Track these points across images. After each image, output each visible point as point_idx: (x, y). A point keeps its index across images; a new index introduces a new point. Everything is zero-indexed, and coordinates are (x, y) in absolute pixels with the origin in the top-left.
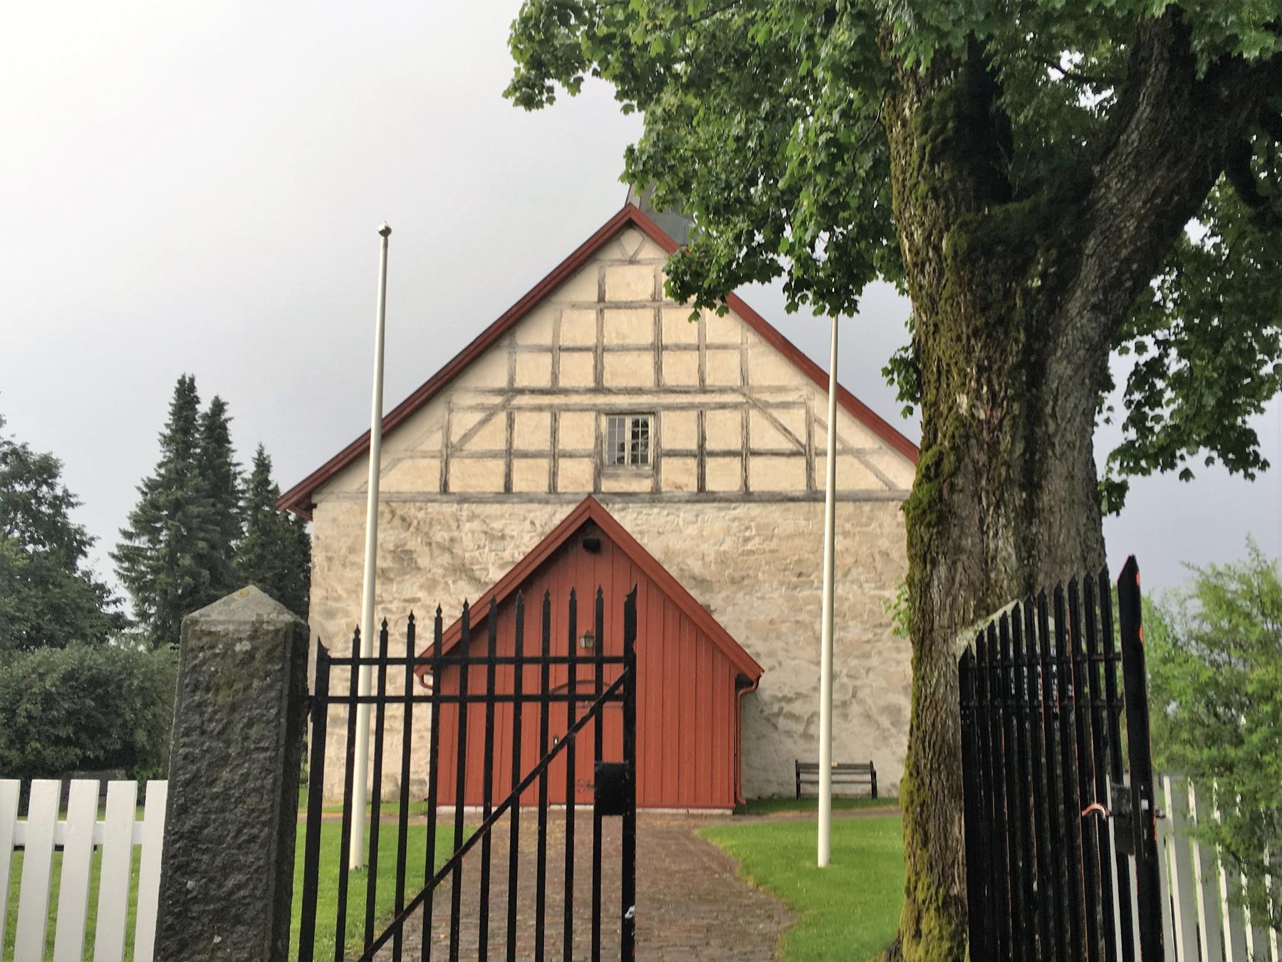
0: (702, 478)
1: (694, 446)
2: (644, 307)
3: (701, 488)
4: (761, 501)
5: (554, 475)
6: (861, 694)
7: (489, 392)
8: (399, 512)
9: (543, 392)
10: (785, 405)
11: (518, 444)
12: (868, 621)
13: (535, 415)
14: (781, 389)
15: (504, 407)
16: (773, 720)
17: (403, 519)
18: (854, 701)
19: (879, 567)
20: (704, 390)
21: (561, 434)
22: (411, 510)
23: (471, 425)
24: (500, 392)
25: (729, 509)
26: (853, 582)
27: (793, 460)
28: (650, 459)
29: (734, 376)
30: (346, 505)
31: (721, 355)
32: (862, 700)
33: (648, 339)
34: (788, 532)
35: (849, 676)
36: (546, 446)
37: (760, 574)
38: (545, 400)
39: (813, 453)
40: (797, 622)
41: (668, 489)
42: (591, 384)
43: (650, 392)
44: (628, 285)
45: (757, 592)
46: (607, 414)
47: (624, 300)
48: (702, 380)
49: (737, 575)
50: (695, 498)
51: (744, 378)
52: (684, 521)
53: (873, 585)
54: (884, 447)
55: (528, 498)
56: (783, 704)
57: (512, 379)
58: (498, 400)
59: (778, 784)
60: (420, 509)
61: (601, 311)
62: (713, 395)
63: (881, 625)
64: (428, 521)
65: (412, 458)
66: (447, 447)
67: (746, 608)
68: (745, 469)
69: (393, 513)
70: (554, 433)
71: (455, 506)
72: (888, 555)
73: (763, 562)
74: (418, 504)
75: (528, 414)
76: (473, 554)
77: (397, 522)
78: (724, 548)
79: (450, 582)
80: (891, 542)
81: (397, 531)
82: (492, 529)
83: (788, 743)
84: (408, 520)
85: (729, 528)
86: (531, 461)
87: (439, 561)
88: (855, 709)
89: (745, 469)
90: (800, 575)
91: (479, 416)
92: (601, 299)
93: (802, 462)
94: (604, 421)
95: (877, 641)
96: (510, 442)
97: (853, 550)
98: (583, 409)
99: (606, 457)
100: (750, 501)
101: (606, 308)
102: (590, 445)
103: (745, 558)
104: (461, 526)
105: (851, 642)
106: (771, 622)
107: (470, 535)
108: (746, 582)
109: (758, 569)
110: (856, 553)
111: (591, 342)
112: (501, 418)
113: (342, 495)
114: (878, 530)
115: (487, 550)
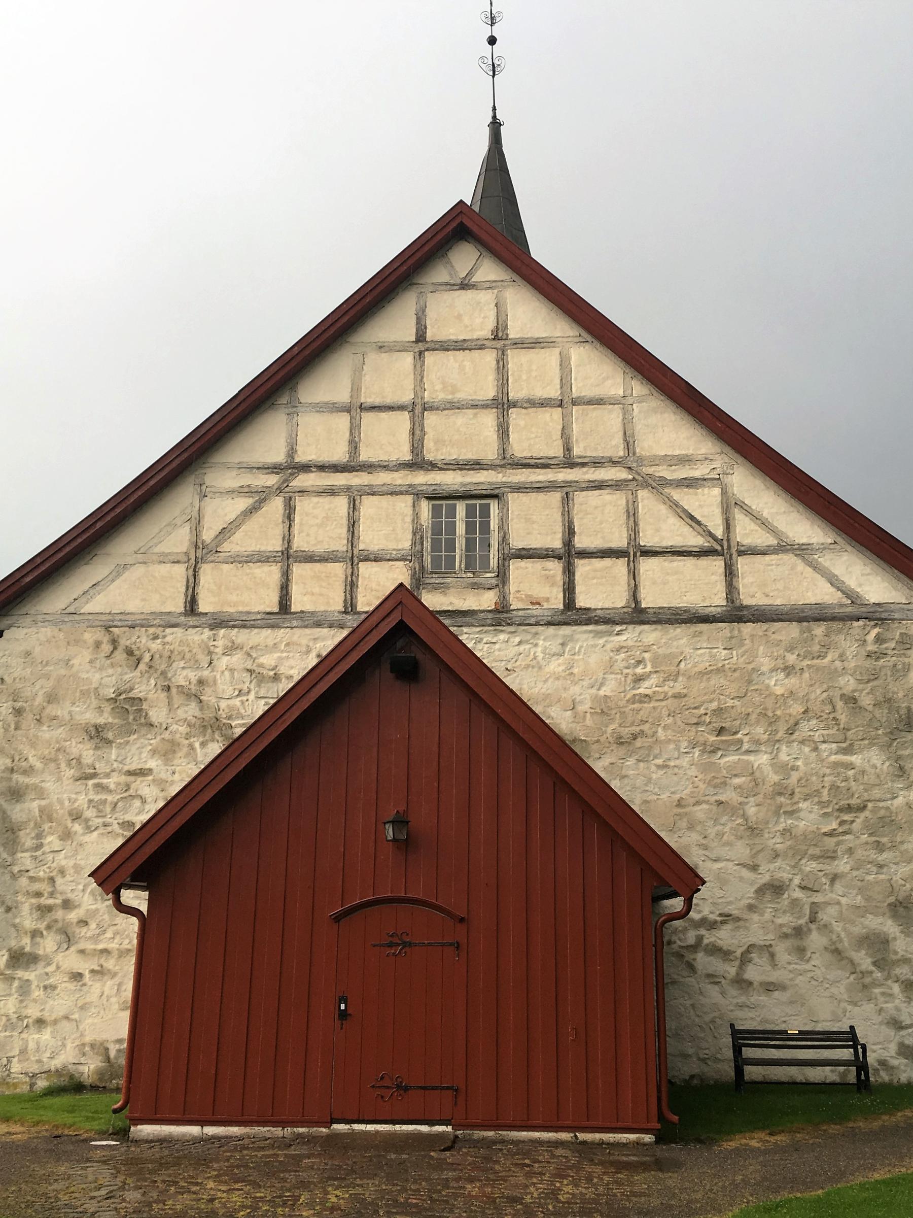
0: (569, 589)
1: (556, 543)
2: (481, 348)
3: (569, 602)
4: (659, 622)
5: (351, 586)
6: (824, 916)
7: (258, 468)
8: (123, 642)
9: (336, 468)
10: (690, 483)
11: (300, 543)
12: (829, 802)
13: (325, 501)
14: (685, 460)
15: (280, 490)
16: (689, 957)
17: (130, 652)
18: (813, 926)
19: (843, 719)
20: (570, 463)
21: (363, 527)
22: (142, 640)
23: (232, 516)
24: (275, 469)
25: (610, 634)
26: (802, 742)
27: (704, 562)
28: (493, 562)
29: (614, 443)
30: (46, 632)
31: (595, 412)
32: (825, 926)
33: (489, 392)
34: (701, 667)
35: (803, 888)
36: (341, 545)
37: (660, 730)
38: (340, 480)
39: (734, 551)
40: (720, 803)
41: (520, 606)
42: (408, 457)
43: (491, 467)
44: (459, 317)
45: (655, 757)
46: (429, 498)
47: (453, 338)
48: (568, 449)
49: (626, 732)
50: (561, 618)
51: (629, 443)
52: (544, 652)
53: (834, 746)
54: (839, 539)
55: (316, 621)
56: (703, 932)
57: (292, 451)
58: (272, 480)
59: (699, 1059)
60: (156, 637)
61: (421, 353)
62: (585, 469)
63: (849, 809)
64: (167, 654)
65: (145, 563)
66: (196, 547)
67: (639, 782)
68: (633, 574)
69: (114, 642)
70: (353, 525)
71: (207, 633)
72: (855, 700)
73: (665, 712)
74: (152, 630)
75: (315, 500)
76: (230, 702)
77: (120, 655)
78: (605, 691)
79: (197, 745)
80: (859, 681)
81: (119, 669)
82: (261, 666)
83: (713, 992)
84: (137, 653)
85: (611, 663)
86: (318, 566)
87: (181, 714)
88: (816, 940)
89: (633, 574)
90: (721, 731)
91: (243, 503)
92: (421, 337)
93: (717, 565)
94: (425, 507)
95: (845, 833)
96: (288, 539)
97: (801, 695)
98: (395, 492)
99: (428, 560)
100: (643, 623)
101: (427, 350)
102: (406, 543)
103: (636, 706)
104: (215, 662)
105: (804, 835)
106: (679, 804)
107: (227, 673)
108: (639, 743)
109: (656, 724)
110: (806, 699)
111: (407, 397)
112: (277, 505)
113: (40, 618)
114: (838, 664)
115: (252, 696)
